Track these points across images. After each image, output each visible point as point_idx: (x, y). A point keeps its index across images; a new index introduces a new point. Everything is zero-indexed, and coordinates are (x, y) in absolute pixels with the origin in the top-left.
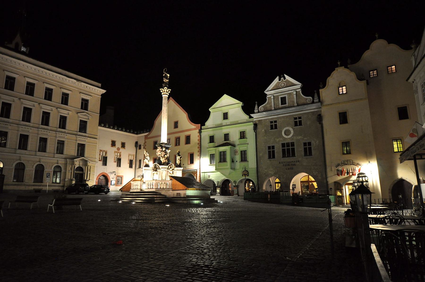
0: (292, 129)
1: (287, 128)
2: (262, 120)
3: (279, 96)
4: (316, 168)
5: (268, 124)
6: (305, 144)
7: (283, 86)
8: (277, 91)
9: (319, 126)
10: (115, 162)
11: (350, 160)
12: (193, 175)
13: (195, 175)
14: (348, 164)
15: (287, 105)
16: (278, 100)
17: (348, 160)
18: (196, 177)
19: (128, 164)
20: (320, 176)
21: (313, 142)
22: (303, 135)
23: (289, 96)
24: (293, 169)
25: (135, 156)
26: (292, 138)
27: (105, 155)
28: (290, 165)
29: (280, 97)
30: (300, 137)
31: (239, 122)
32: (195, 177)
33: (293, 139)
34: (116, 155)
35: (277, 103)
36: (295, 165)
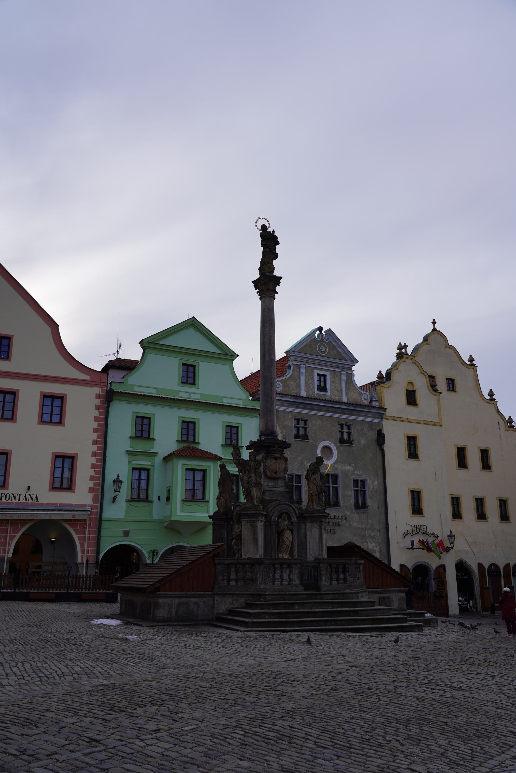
0: (335, 448)
1: (327, 443)
3: (315, 370)
4: (372, 535)
5: (289, 425)
6: (356, 481)
7: (324, 352)
9: (379, 453)
15: (329, 393)
16: (313, 378)
17: (420, 525)
20: (379, 552)
21: (369, 482)
22: (353, 465)
23: (333, 378)
24: (334, 533)
26: (334, 466)
28: (330, 524)
29: (316, 372)
30: (348, 468)
31: (226, 402)
33: (336, 469)
36: (338, 525)
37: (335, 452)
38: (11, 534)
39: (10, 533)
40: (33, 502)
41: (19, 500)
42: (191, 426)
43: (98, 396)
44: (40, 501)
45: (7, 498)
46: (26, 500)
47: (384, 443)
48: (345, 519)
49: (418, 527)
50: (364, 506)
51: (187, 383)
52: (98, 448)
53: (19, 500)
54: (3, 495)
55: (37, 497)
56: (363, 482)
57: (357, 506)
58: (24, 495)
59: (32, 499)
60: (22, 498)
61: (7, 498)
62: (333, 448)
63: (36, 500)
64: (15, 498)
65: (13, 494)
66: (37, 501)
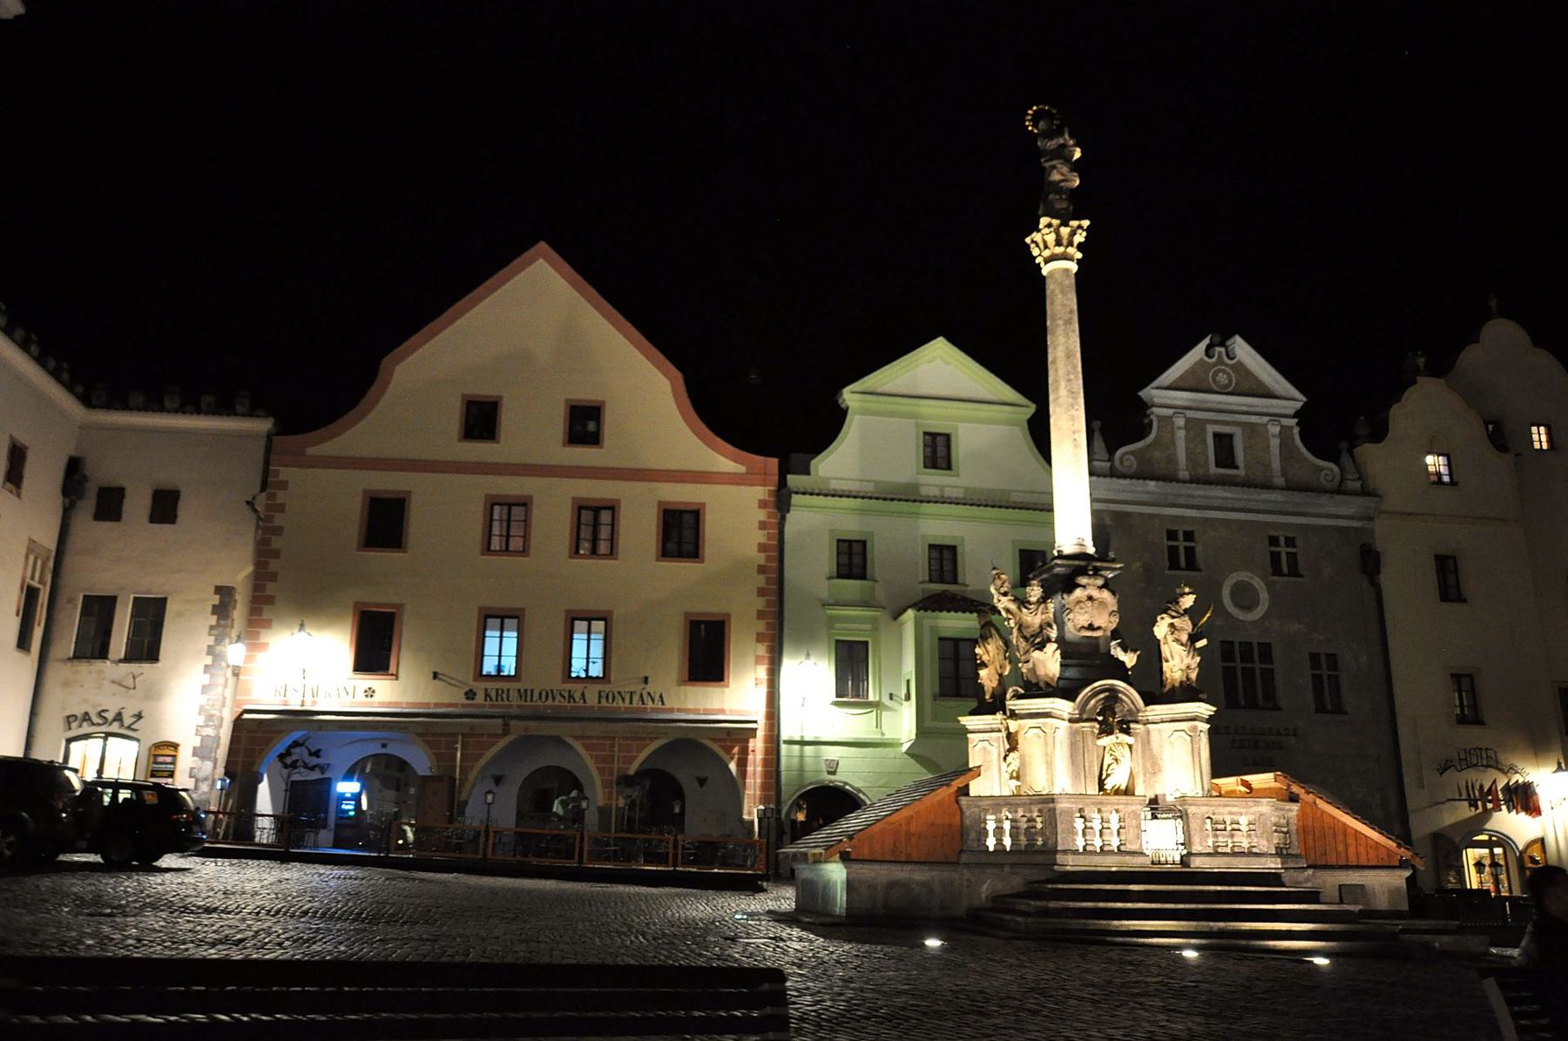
0: (1263, 585)
1: (1243, 576)
2: (1129, 514)
3: (1207, 426)
6: (1315, 658)
8: (1219, 403)
11: (1487, 749)
12: (722, 753)
13: (736, 750)
14: (1480, 764)
16: (1204, 441)
17: (1480, 749)
18: (738, 765)
19: (17, 615)
23: (1250, 439)
25: (51, 564)
29: (1211, 429)
30: (1295, 627)
32: (733, 766)
35: (1198, 451)
37: (1264, 596)
38: (621, 766)
39: (618, 763)
40: (656, 706)
41: (631, 703)
42: (947, 555)
43: (763, 504)
44: (668, 705)
45: (610, 701)
46: (643, 703)
47: (1379, 572)
48: (1295, 735)
49: (1472, 752)
50: (1339, 710)
51: (935, 466)
52: (769, 603)
53: (631, 703)
54: (602, 694)
55: (661, 696)
56: (1332, 658)
57: (1321, 709)
58: (639, 694)
59: (653, 701)
60: (636, 698)
61: (610, 701)
62: (1257, 587)
63: (660, 703)
64: (623, 699)
65: (619, 693)
66: (663, 704)
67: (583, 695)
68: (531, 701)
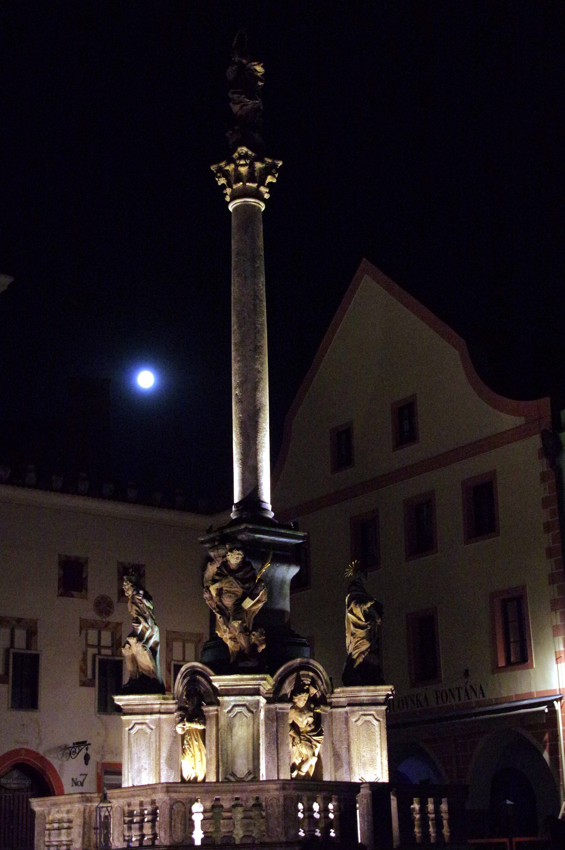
10: (84, 684)
12: (534, 741)
13: (547, 737)
18: (551, 754)
27: (28, 647)
32: (546, 755)
34: (90, 642)
41: (460, 700)
46: (469, 699)
53: (460, 700)
55: (481, 688)
63: (481, 697)
66: (484, 696)
67: (426, 697)
68: (394, 711)
